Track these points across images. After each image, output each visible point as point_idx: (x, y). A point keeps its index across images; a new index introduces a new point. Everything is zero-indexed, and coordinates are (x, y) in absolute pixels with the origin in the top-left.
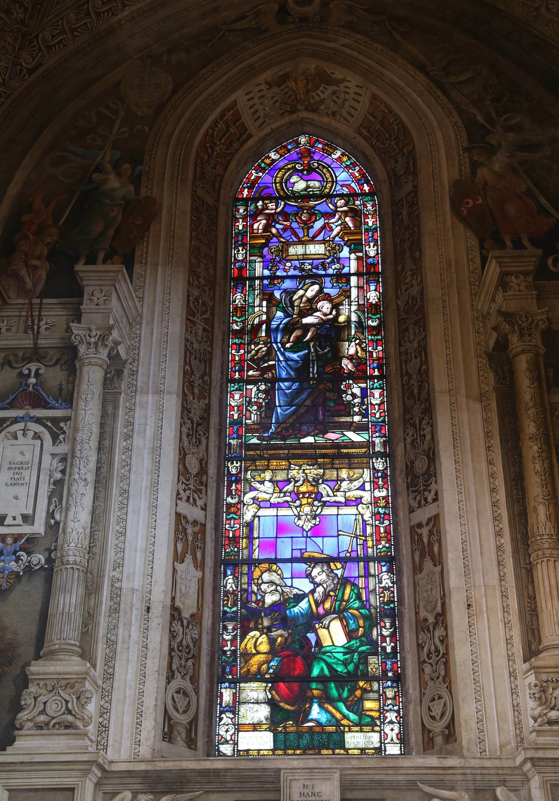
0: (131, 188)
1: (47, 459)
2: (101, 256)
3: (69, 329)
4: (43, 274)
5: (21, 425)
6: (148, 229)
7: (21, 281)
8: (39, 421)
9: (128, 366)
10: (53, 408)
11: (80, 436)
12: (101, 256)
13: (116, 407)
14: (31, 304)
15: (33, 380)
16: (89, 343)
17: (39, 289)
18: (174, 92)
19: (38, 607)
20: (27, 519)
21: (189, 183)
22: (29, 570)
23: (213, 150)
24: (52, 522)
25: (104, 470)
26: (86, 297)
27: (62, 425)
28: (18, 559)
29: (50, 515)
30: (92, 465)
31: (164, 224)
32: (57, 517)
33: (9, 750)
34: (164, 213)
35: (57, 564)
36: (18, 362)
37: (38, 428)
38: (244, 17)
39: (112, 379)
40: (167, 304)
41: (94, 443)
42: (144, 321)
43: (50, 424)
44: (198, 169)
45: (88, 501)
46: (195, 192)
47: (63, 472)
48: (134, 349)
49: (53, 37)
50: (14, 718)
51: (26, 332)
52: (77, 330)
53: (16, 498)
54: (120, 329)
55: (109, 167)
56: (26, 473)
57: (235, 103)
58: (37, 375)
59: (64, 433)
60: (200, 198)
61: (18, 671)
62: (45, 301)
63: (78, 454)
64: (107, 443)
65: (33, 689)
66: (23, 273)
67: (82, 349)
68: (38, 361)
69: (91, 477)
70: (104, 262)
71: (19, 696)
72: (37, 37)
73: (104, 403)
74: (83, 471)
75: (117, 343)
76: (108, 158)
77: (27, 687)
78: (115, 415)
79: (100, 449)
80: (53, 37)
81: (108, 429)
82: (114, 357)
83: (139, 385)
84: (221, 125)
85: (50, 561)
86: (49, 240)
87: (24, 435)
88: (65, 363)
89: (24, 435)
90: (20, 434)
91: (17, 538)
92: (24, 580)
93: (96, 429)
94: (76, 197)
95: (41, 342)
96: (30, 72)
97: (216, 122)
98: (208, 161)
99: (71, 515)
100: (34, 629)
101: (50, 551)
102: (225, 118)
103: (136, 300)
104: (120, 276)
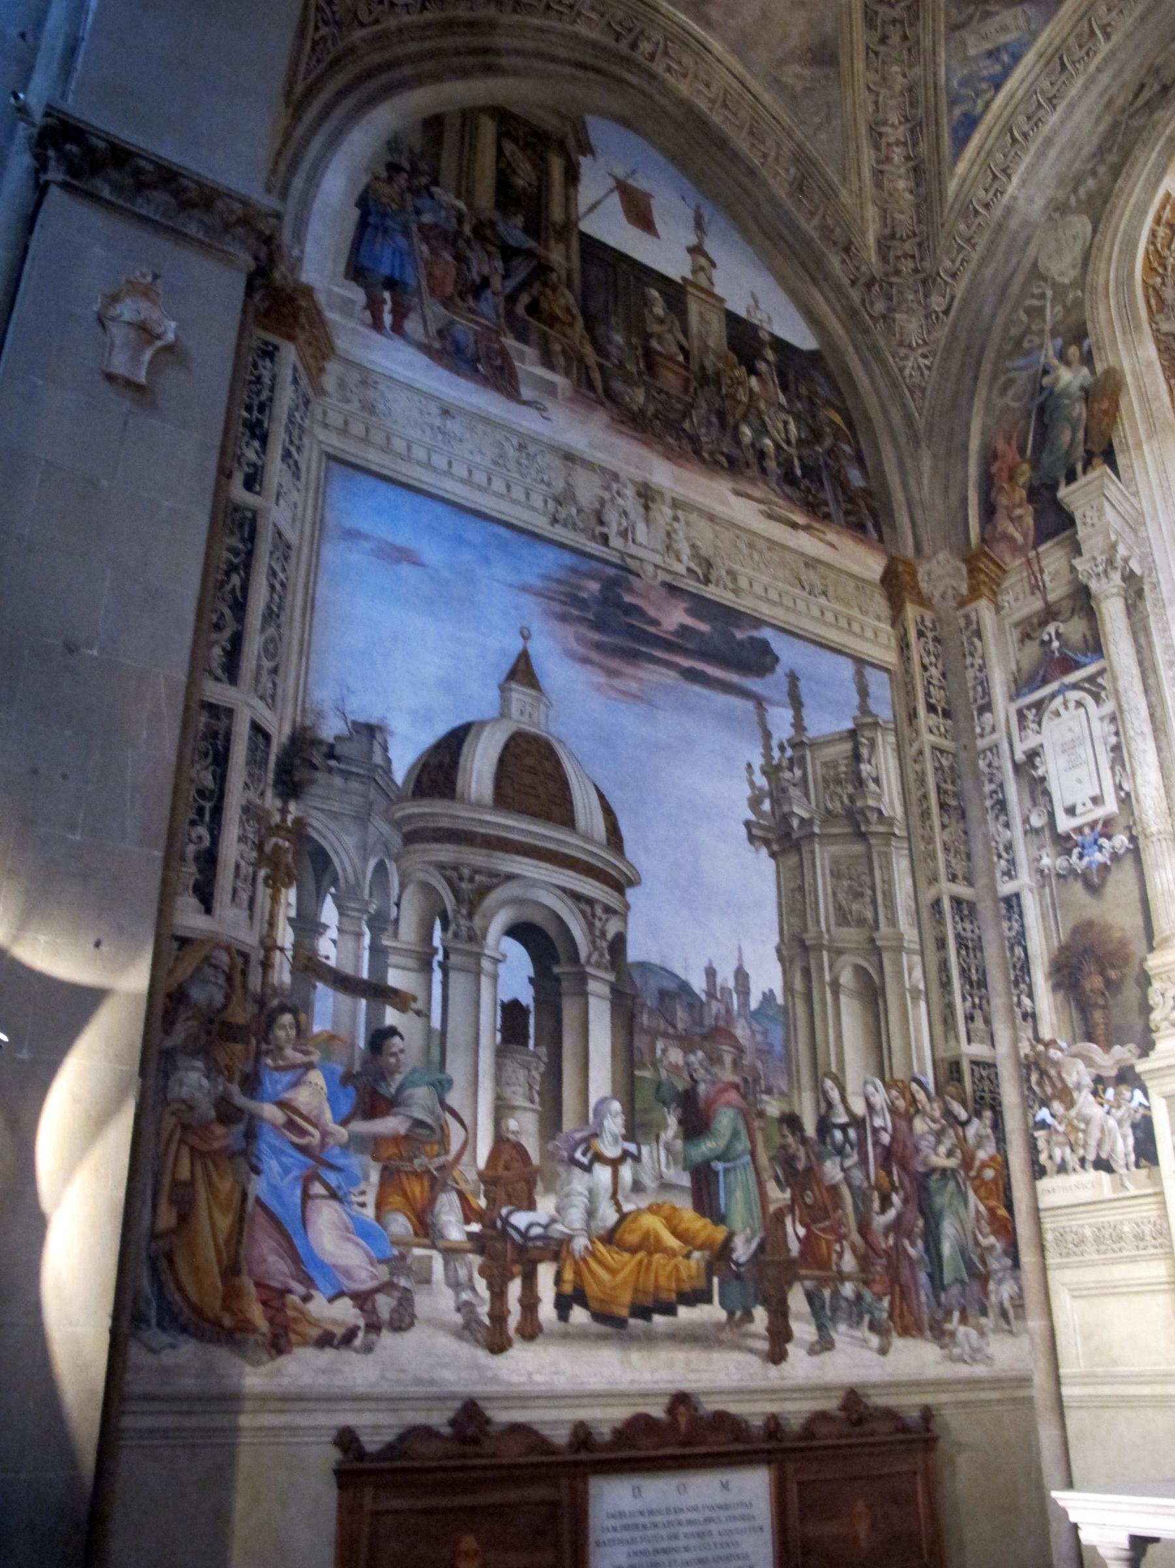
0: (1085, 371)
1: (1096, 725)
2: (1079, 467)
3: (1073, 569)
4: (1029, 521)
5: (1059, 700)
6: (1117, 407)
7: (1011, 539)
8: (1075, 686)
9: (1147, 580)
10: (1085, 665)
11: (1122, 685)
12: (1079, 467)
13: (1148, 634)
14: (1029, 561)
15: (1056, 644)
16: (1098, 575)
17: (1031, 539)
18: (1095, 231)
19: (1136, 895)
20: (1096, 800)
21: (1145, 325)
22: (1115, 857)
23: (1165, 267)
24: (1122, 794)
25: (1158, 714)
26: (1078, 521)
27: (1100, 680)
28: (1101, 848)
29: (1119, 787)
30: (1144, 713)
31: (1133, 392)
32: (1126, 786)
33: (1152, 1054)
34: (1129, 380)
35: (1141, 842)
36: (1034, 630)
37: (1074, 695)
38: (1142, 87)
39: (1135, 605)
40: (1165, 484)
41: (1138, 687)
42: (1148, 519)
43: (1087, 685)
44: (1153, 302)
45: (1152, 758)
46: (1158, 330)
47: (1117, 734)
48: (1147, 558)
49: (953, 261)
50: (1147, 1020)
51: (1033, 593)
52: (1081, 564)
53: (1079, 781)
54: (1124, 541)
55: (1055, 362)
56: (1080, 751)
57: (1168, 196)
58: (1058, 635)
59: (1104, 688)
60: (1167, 334)
61: (1137, 970)
62: (1041, 549)
63: (1125, 706)
64: (1151, 681)
65: (1157, 985)
66: (1011, 530)
67: (1094, 585)
68: (1054, 619)
69: (1147, 728)
70: (1085, 472)
71: (1145, 997)
72: (938, 274)
73: (1135, 634)
74: (1136, 723)
75: (1126, 560)
76: (1051, 352)
77: (1150, 984)
78: (1150, 644)
79: (1147, 690)
80: (953, 261)
81: (1147, 664)
82: (1129, 577)
83: (1165, 596)
84: (1162, 232)
85: (1133, 839)
86: (1022, 480)
87: (1066, 708)
88: (1082, 609)
89: (1066, 708)
90: (1062, 710)
91: (1093, 825)
92: (1114, 869)
93: (1135, 671)
94: (1034, 416)
95: (1052, 597)
96: (946, 312)
97: (1153, 234)
98: (1163, 283)
99: (1139, 780)
100: (1139, 920)
101: (1129, 828)
102: (1164, 220)
103: (1131, 498)
104: (1106, 480)
